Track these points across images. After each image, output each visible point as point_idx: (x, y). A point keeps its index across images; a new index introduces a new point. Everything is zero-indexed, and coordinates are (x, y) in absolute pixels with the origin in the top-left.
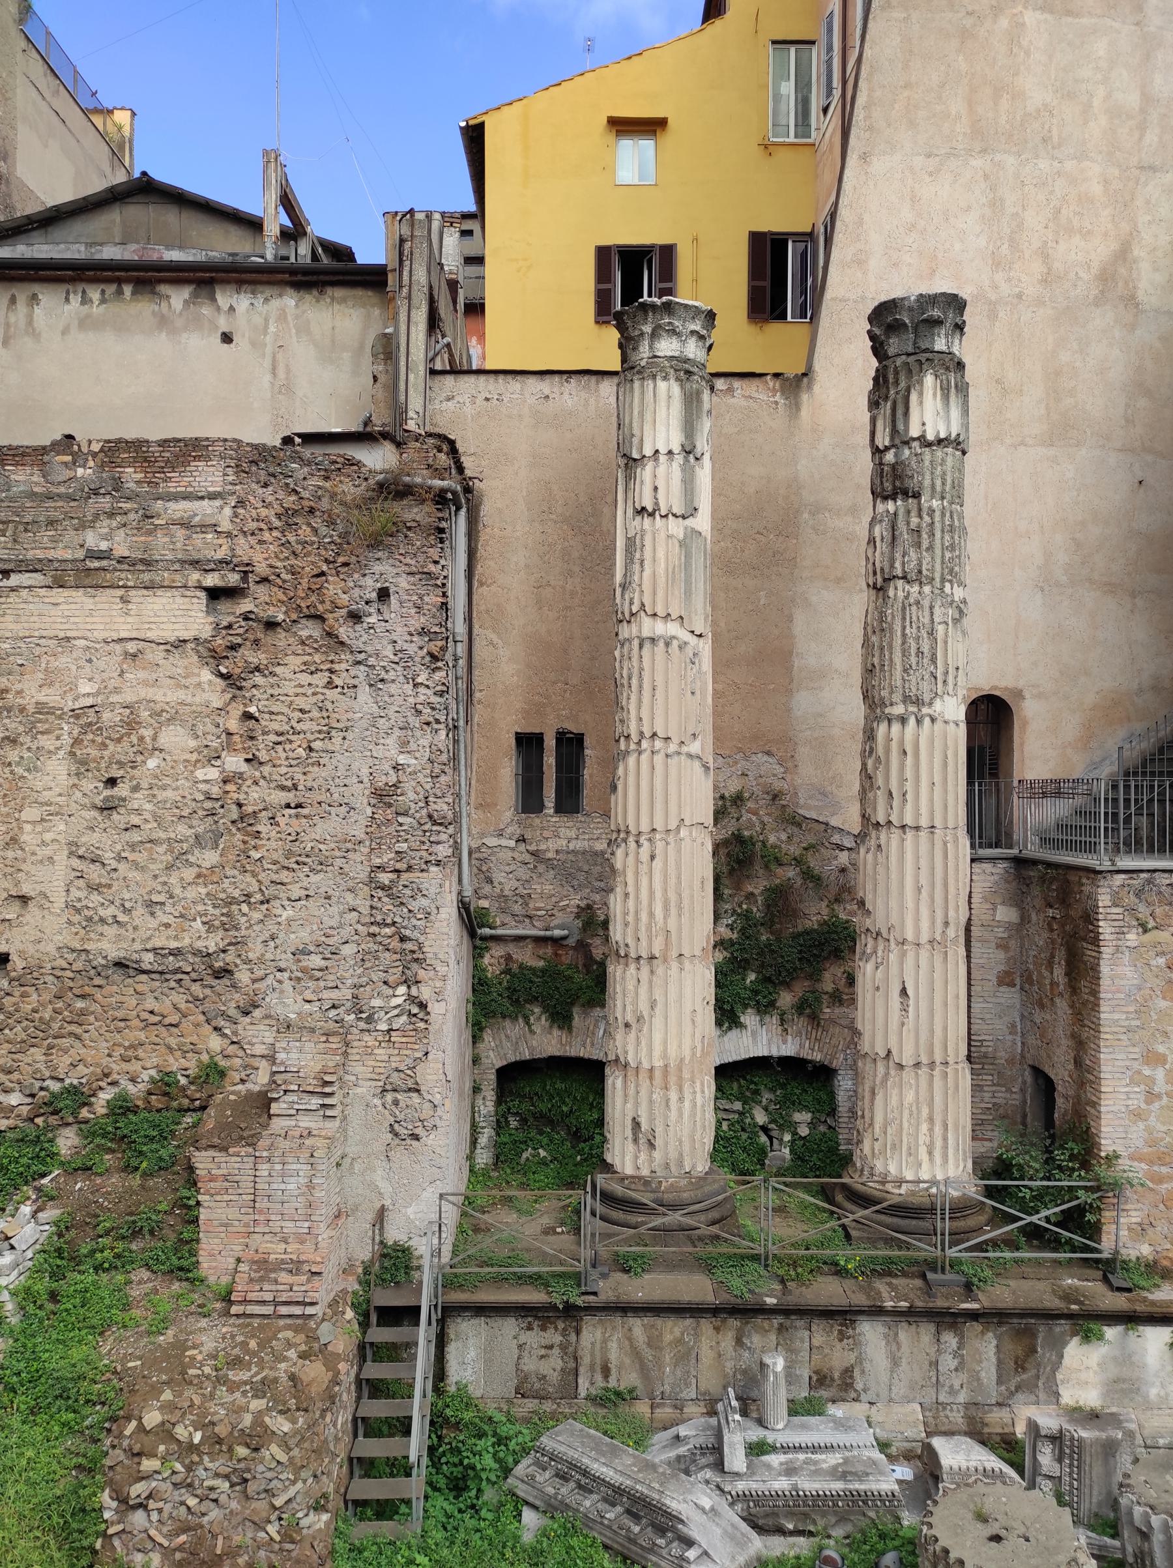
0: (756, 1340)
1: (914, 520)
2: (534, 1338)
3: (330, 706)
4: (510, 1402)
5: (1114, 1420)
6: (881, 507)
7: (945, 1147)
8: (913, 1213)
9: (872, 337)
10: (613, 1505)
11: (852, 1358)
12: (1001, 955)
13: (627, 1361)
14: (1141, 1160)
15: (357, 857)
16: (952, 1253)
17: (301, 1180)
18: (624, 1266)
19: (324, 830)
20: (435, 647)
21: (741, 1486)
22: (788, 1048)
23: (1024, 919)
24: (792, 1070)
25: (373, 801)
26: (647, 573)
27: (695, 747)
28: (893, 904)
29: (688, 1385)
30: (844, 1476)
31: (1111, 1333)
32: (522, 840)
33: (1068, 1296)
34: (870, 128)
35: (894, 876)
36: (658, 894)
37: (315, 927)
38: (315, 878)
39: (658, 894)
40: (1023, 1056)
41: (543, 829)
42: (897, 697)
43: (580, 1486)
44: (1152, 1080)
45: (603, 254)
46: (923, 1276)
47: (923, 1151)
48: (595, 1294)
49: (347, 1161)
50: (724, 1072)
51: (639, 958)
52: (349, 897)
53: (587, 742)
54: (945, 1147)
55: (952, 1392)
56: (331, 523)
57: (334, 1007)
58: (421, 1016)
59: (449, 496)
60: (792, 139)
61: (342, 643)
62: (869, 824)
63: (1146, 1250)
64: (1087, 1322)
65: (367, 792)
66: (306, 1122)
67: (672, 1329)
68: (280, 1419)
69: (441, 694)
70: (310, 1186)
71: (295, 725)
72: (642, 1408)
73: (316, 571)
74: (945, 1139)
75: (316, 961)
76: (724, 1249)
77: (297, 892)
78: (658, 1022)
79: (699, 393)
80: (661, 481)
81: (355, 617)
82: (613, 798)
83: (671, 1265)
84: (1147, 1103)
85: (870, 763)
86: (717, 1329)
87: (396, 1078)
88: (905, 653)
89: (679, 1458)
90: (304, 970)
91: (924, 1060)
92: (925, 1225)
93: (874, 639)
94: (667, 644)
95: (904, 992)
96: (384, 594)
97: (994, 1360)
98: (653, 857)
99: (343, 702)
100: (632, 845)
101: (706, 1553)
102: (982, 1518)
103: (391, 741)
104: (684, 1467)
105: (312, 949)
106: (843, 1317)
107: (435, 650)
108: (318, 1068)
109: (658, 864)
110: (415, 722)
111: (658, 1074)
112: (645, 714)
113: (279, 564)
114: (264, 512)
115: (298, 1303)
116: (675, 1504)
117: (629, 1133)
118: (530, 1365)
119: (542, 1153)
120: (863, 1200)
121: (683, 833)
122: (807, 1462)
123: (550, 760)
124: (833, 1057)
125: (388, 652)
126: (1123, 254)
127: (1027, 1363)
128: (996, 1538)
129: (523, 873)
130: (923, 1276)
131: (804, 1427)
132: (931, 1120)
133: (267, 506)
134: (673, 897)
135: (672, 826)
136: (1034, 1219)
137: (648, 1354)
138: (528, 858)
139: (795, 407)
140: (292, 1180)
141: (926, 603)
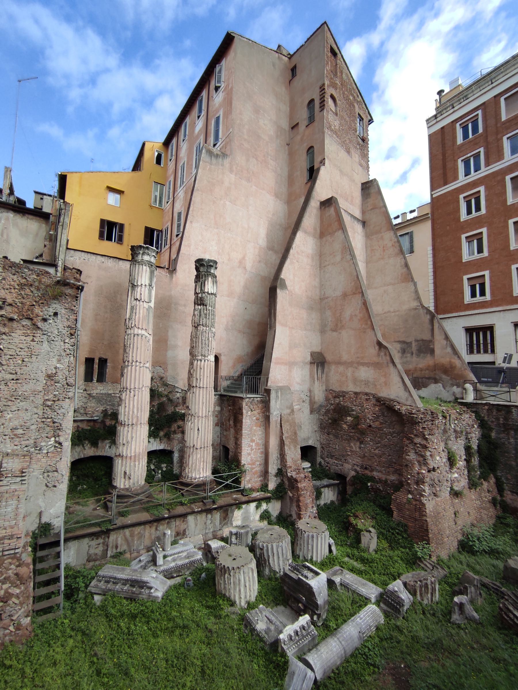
0: (161, 528)
1: (205, 311)
2: (94, 543)
3: (32, 348)
4: (84, 565)
5: (247, 526)
6: (197, 307)
7: (206, 468)
8: (201, 486)
9: (196, 265)
10: (126, 585)
11: (186, 526)
12: (216, 419)
13: (123, 542)
14: (249, 464)
15: (39, 396)
16: (209, 494)
17: (13, 507)
18: (122, 514)
19: (26, 388)
20: (72, 332)
21: (162, 568)
22: (161, 447)
23: (222, 409)
24: (162, 452)
25: (46, 378)
26: (137, 316)
27: (147, 365)
28: (197, 407)
29: (141, 545)
30: (188, 558)
31: (244, 506)
32: (85, 390)
33: (235, 499)
34: (193, 216)
35: (197, 400)
36: (136, 406)
37: (21, 420)
38: (21, 404)
39: (136, 406)
40: (220, 443)
41: (92, 387)
42: (199, 354)
43: (114, 583)
44: (252, 445)
45: (102, 221)
46: (203, 502)
47: (201, 469)
48: (116, 524)
49: (28, 498)
50: (151, 454)
51: (128, 425)
52: (35, 410)
53: (108, 361)
54: (206, 468)
55: (209, 529)
56: (38, 289)
57: (26, 446)
58: (59, 447)
59: (81, 287)
60: (157, 206)
61: (39, 328)
62: (190, 386)
63: (250, 486)
64: (238, 505)
65: (44, 376)
66: (13, 487)
67: (137, 530)
68: (15, 589)
69: (72, 346)
70: (17, 508)
71: (18, 353)
72: (128, 555)
73: (31, 304)
74: (206, 466)
75: (20, 431)
76: (151, 504)
77: (14, 408)
78: (133, 443)
79: (154, 271)
80: (142, 292)
81: (45, 320)
82: (122, 378)
83: (135, 512)
84: (251, 451)
85: (192, 371)
86: (150, 527)
87: (49, 468)
88: (202, 344)
89: (141, 566)
90: (15, 435)
91: (203, 446)
92: (202, 488)
93: (194, 339)
94: (142, 336)
95: (198, 429)
96: (56, 314)
97: (219, 519)
98: (134, 396)
99: (37, 346)
100: (128, 392)
101: (156, 589)
102: (230, 555)
103: (55, 360)
104: (144, 568)
105: (19, 427)
106: (184, 516)
107: (72, 333)
108: (20, 467)
109: (136, 398)
110: (64, 354)
111: (133, 458)
112: (134, 355)
113: (17, 300)
114: (12, 283)
115: (12, 549)
116: (145, 578)
117: (123, 476)
118: (92, 551)
119: (85, 487)
120: (187, 485)
121: (143, 389)
122: (178, 557)
123: (96, 366)
124: (173, 448)
125: (56, 332)
126: (244, 258)
127: (226, 518)
128: (234, 559)
129: (85, 400)
130: (203, 502)
131: (175, 548)
132: (204, 461)
133: (15, 281)
134: (139, 406)
135: (140, 387)
136: (228, 482)
137: (130, 539)
138: (87, 395)
139: (172, 277)
140: (9, 507)
141: (207, 332)
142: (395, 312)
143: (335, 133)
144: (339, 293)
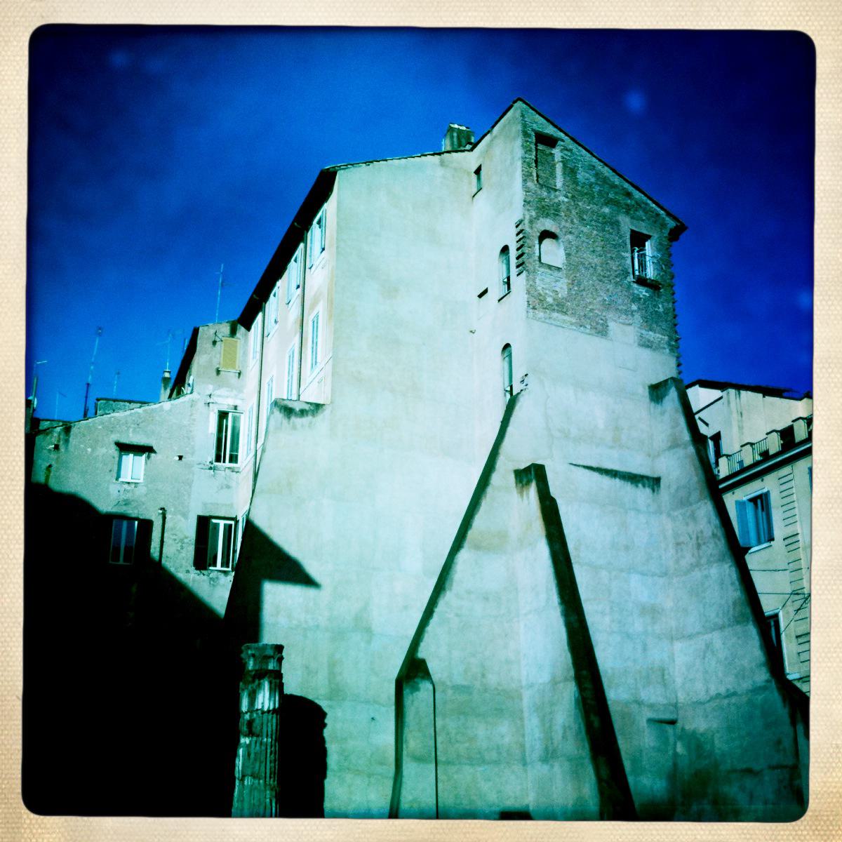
142: (727, 696)
143: (560, 307)
144: (545, 677)
